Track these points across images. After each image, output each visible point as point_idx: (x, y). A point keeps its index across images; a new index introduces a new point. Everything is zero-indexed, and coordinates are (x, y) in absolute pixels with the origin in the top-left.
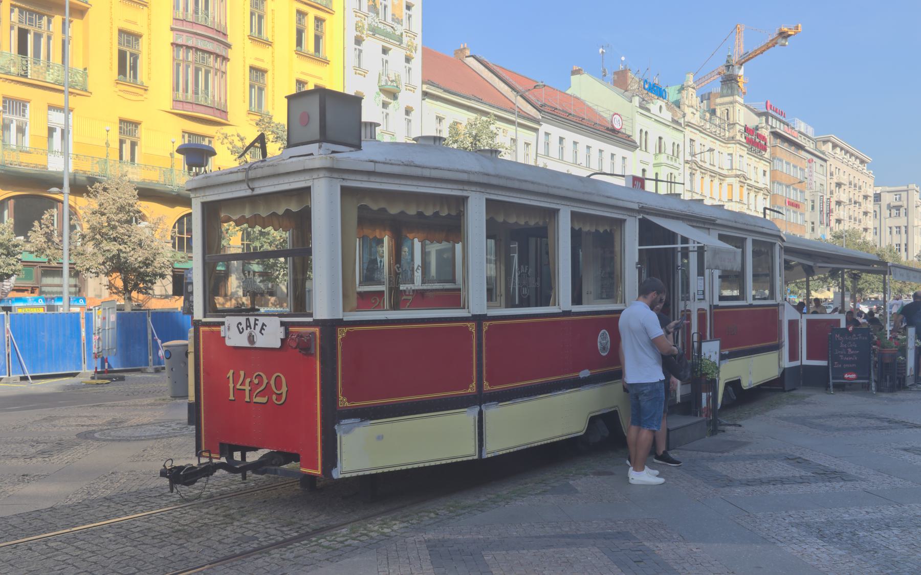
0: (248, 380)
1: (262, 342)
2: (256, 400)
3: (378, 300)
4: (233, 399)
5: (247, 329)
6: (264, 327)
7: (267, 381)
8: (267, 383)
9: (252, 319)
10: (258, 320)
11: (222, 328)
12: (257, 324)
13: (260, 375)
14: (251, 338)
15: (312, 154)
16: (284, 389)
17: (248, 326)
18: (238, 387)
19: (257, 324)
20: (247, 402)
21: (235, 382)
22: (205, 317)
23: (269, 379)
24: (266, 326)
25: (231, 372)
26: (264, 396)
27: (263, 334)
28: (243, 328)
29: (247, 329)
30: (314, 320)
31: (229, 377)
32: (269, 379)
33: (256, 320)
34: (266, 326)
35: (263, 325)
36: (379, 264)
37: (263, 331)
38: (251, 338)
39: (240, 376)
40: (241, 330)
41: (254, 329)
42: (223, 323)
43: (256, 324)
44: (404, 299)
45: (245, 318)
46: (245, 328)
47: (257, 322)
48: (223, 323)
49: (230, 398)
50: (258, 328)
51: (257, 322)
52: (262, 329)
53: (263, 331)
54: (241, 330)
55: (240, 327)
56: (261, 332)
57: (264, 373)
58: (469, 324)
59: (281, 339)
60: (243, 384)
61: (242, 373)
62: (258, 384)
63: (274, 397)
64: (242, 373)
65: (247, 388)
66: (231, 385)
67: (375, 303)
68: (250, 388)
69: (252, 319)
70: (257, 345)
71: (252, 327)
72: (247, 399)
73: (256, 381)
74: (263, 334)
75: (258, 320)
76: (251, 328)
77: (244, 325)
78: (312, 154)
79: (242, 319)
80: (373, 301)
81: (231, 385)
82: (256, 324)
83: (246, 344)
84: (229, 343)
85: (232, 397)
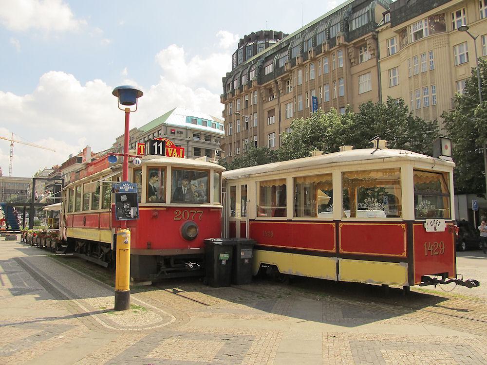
9: (436, 220)
14: (435, 228)
16: (444, 248)
23: (439, 244)
25: (426, 243)
32: (439, 244)
36: (183, 191)
38: (435, 228)
39: (429, 244)
48: (425, 222)
50: (438, 223)
58: (333, 224)
63: (441, 251)
65: (431, 249)
66: (426, 249)
70: (437, 231)
79: (432, 220)
84: (427, 230)
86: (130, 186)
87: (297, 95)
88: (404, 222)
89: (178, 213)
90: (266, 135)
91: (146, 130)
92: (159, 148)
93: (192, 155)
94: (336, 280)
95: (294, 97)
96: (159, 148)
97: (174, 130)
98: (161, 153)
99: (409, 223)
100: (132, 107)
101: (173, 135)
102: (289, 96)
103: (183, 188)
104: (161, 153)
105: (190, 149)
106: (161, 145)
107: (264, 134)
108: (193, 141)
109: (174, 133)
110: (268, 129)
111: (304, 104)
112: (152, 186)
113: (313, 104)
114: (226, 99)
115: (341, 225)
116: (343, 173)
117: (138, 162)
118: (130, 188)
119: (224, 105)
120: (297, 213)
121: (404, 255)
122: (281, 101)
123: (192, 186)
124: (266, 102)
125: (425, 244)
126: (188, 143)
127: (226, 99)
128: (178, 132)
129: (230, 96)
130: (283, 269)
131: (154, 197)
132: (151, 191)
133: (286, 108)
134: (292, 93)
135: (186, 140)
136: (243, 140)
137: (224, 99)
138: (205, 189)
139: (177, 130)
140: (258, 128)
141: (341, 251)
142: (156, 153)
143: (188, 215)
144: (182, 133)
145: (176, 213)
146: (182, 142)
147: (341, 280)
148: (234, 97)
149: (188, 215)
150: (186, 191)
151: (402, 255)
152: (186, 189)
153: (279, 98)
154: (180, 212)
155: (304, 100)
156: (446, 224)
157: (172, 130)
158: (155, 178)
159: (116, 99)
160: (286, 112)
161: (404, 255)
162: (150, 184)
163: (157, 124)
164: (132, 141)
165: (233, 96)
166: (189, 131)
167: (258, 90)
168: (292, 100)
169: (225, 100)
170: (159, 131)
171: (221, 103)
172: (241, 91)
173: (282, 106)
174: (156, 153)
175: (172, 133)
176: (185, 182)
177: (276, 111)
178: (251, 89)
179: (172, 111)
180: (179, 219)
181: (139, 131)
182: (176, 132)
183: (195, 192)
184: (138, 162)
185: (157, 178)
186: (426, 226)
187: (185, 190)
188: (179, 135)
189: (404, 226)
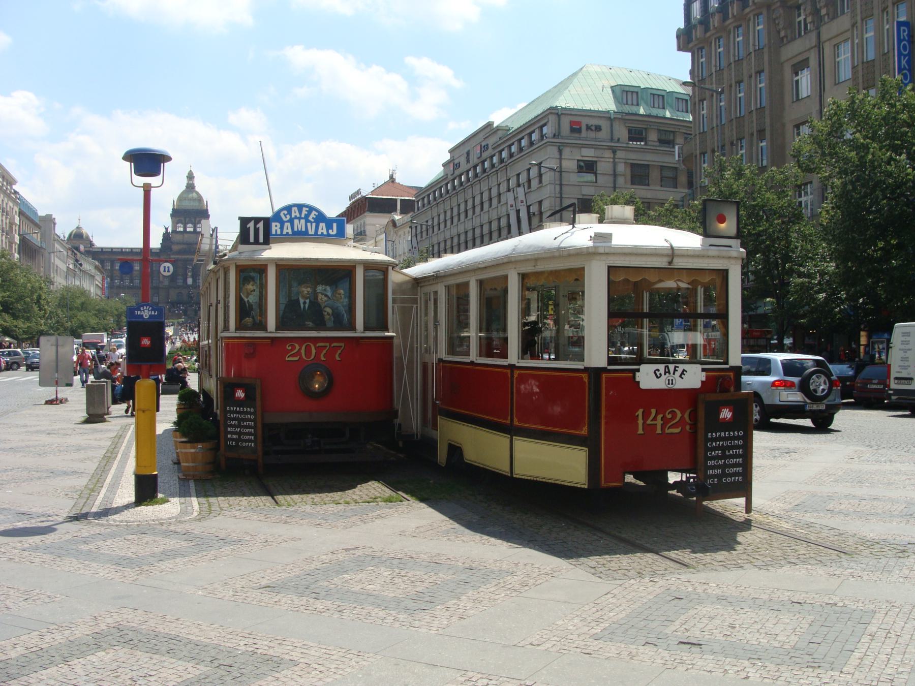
0: (660, 417)
1: (680, 384)
2: (667, 431)
3: (297, 345)
4: (642, 433)
5: (665, 374)
6: (685, 372)
7: (681, 415)
8: (681, 417)
9: (672, 367)
10: (678, 367)
11: (637, 374)
12: (677, 371)
13: (674, 411)
15: (730, 246)
17: (667, 371)
18: (649, 422)
19: (677, 371)
20: (658, 434)
21: (646, 416)
22: (609, 364)
23: (683, 413)
24: (686, 372)
26: (678, 428)
27: (682, 378)
28: (661, 374)
29: (665, 374)
30: (731, 367)
31: (638, 416)
33: (676, 367)
34: (686, 372)
35: (684, 370)
36: (302, 306)
37: (683, 376)
38: (671, 382)
39: (650, 413)
40: (659, 376)
41: (674, 374)
42: (638, 370)
43: (675, 370)
44: (319, 346)
45: (664, 365)
46: (663, 374)
47: (677, 369)
49: (638, 433)
50: (678, 374)
51: (677, 369)
52: (682, 373)
53: (683, 376)
54: (659, 376)
55: (658, 373)
56: (680, 376)
57: (679, 410)
59: (702, 382)
60: (655, 419)
61: (653, 411)
62: (671, 418)
64: (653, 411)
65: (659, 422)
66: (640, 421)
67: (292, 350)
68: (662, 422)
69: (672, 367)
71: (672, 372)
72: (659, 431)
73: (669, 416)
74: (682, 378)
75: (678, 367)
76: (670, 374)
77: (662, 372)
78: (730, 246)
79: (662, 367)
80: (290, 348)
81: (640, 421)
82: (675, 370)
83: (664, 387)
84: (644, 385)
85: (640, 431)
86: (151, 310)
87: (859, 18)
88: (586, 370)
89: (294, 348)
90: (789, 128)
91: (515, 125)
92: (257, 231)
93: (626, 182)
94: (509, 475)
95: (854, 25)
96: (257, 231)
97: (579, 123)
98: (261, 240)
99: (596, 373)
100: (153, 181)
101: (577, 135)
102: (843, 22)
103: (302, 301)
104: (261, 240)
105: (621, 168)
106: (261, 225)
107: (783, 125)
108: (628, 149)
109: (579, 131)
110: (792, 113)
111: (879, 44)
112: (246, 300)
113: (899, 41)
114: (689, 40)
115: (517, 372)
116: (611, 269)
117: (167, 269)
118: (153, 313)
119: (688, 55)
120: (529, 346)
121: (584, 431)
122: (824, 37)
123: (320, 296)
124: (789, 42)
125: (640, 412)
126: (614, 152)
127: (689, 40)
128: (588, 128)
129: (698, 33)
130: (471, 455)
131: (248, 320)
132: (243, 310)
133: (836, 55)
134: (849, 14)
135: (610, 148)
136: (732, 144)
137: (685, 40)
138: (347, 300)
139: (585, 121)
140: (767, 112)
141: (516, 422)
142: (252, 240)
143: (314, 351)
144: (598, 128)
145: (290, 348)
146: (599, 153)
147: (515, 476)
148: (708, 34)
149: (314, 351)
150: (307, 306)
151: (583, 432)
152: (308, 301)
153: (818, 28)
154: (297, 345)
155: (879, 29)
156: (704, 374)
157: (572, 123)
158: (250, 287)
159: (127, 166)
160: (836, 66)
161: (584, 431)
162: (243, 296)
163: (539, 111)
164: (486, 155)
165: (707, 30)
166: (616, 126)
167: (765, 12)
168: (849, 34)
169: (689, 43)
170: (541, 128)
171: (679, 49)
172: (725, 18)
173: (828, 49)
174: (252, 240)
175: (573, 130)
176: (306, 290)
177: (813, 62)
178: (747, 10)
179: (575, 75)
180: (296, 359)
181: (498, 129)
182: (584, 128)
183: (325, 307)
184: (167, 269)
185: (253, 285)
186: (639, 377)
187: (305, 303)
188: (592, 134)
189: (585, 376)
